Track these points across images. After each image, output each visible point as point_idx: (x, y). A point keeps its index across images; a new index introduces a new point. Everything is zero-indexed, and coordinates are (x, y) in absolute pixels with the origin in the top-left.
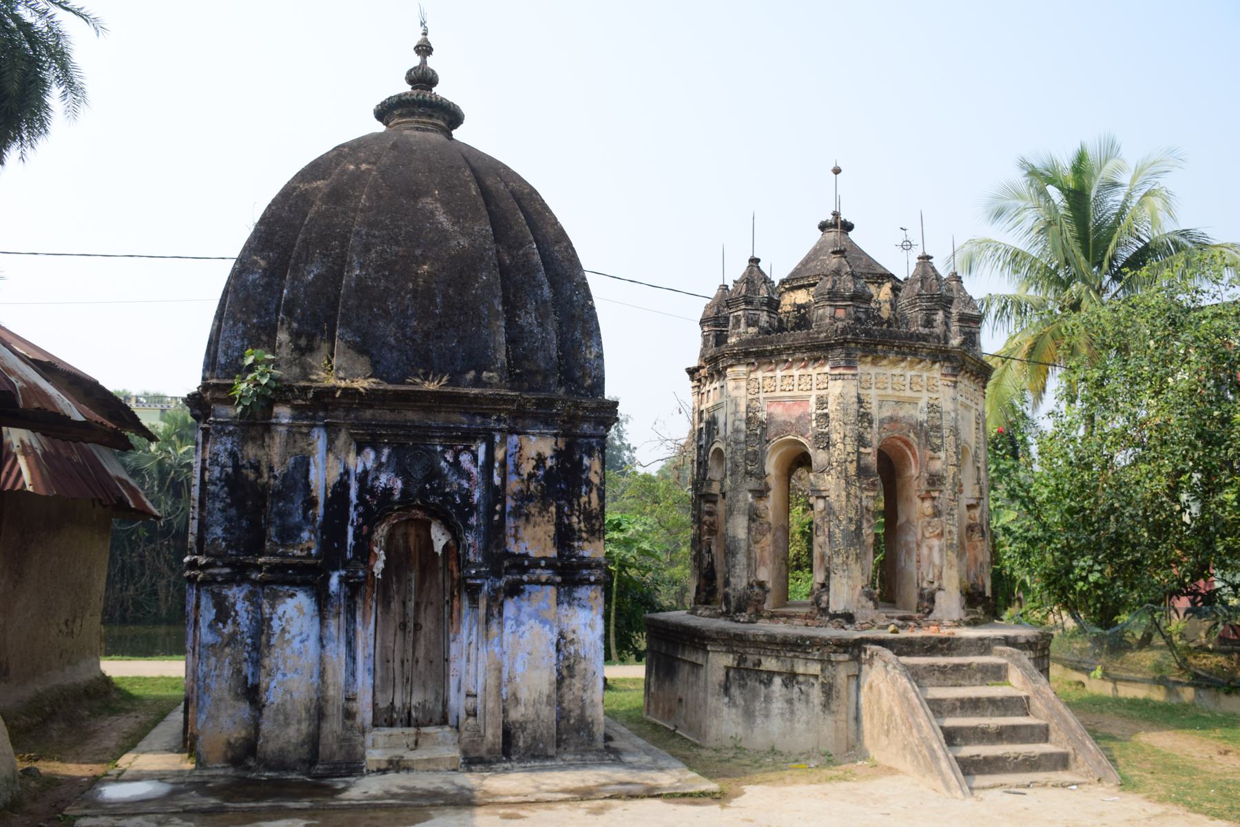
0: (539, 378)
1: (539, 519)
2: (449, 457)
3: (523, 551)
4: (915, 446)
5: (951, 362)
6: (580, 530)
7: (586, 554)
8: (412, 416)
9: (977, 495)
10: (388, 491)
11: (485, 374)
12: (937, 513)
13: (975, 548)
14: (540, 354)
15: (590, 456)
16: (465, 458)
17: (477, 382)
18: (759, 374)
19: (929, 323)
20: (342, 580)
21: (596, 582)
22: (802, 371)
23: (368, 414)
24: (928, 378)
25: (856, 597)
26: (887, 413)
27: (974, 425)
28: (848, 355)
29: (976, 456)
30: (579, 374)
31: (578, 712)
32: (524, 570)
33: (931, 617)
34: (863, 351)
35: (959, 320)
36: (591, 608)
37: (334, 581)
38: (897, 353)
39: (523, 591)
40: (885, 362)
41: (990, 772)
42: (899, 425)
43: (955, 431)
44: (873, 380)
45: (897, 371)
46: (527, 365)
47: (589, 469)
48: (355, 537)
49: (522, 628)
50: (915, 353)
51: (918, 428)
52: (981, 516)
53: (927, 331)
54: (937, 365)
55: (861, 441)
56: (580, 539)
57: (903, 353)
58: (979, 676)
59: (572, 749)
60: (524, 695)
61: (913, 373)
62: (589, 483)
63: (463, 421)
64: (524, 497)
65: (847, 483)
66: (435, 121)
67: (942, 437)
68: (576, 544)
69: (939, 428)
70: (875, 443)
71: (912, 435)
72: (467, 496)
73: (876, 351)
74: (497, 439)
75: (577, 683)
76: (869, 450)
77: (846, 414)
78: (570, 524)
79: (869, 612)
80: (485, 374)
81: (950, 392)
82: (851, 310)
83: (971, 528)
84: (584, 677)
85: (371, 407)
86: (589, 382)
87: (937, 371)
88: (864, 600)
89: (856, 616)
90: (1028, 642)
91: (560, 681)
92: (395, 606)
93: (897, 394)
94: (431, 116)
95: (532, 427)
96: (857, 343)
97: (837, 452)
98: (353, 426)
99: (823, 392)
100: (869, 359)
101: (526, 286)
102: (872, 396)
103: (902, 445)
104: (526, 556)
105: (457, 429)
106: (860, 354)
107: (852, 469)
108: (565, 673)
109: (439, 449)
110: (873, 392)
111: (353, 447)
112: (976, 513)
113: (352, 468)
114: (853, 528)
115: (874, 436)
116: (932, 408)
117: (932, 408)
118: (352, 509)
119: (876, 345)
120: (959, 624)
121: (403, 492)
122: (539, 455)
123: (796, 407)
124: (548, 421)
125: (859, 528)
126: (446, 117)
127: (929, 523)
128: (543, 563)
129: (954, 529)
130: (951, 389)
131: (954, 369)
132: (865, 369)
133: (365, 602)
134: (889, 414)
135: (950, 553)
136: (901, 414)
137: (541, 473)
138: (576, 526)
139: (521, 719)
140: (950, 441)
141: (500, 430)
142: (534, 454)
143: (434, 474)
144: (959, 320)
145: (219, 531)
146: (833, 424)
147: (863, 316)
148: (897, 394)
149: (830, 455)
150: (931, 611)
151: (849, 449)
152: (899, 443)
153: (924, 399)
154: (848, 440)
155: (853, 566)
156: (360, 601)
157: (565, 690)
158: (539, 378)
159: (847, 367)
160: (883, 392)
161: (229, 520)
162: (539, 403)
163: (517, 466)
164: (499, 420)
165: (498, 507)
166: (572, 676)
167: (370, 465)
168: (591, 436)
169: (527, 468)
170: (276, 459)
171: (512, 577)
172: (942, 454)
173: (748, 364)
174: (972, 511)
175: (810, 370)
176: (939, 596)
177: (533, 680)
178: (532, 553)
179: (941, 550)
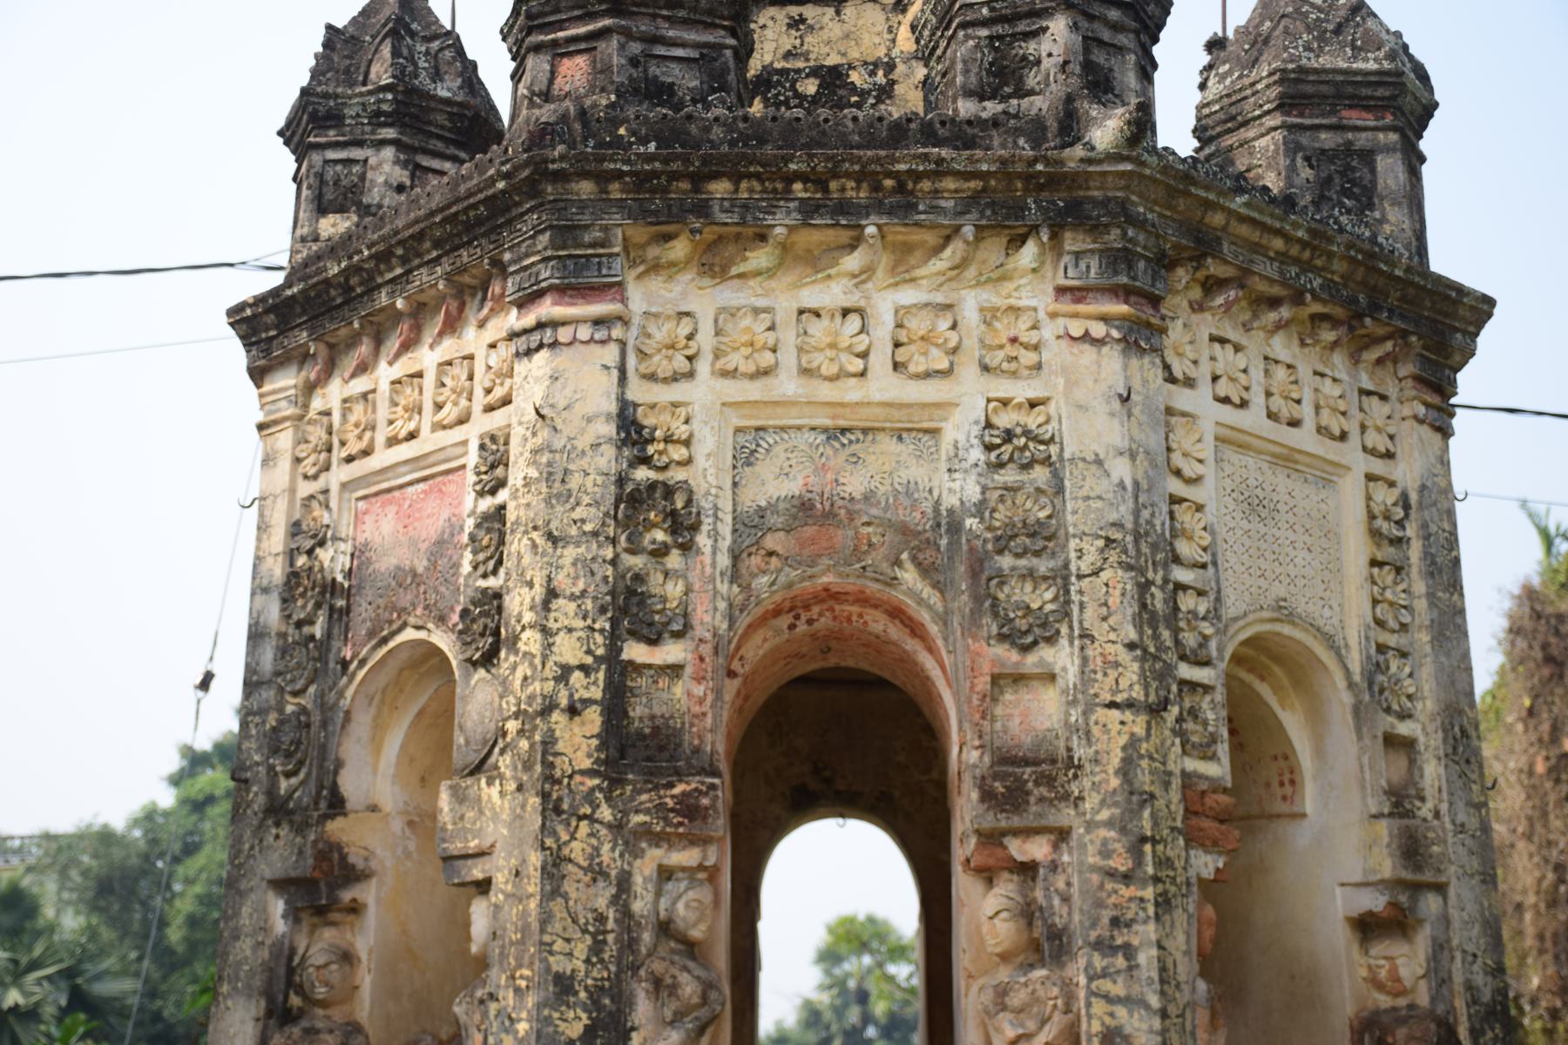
4: (934, 629)
5: (1096, 229)
9: (1387, 867)
12: (1045, 944)
18: (333, 394)
19: (1004, 75)
22: (449, 348)
24: (989, 315)
26: (776, 482)
27: (1356, 550)
28: (566, 233)
29: (1376, 690)
34: (641, 214)
35: (1283, 106)
38: (809, 210)
40: (760, 258)
42: (843, 537)
43: (1150, 548)
44: (705, 339)
45: (830, 293)
50: (900, 201)
51: (933, 540)
52: (1437, 973)
53: (992, 108)
54: (1028, 253)
55: (631, 610)
65: (552, 808)
67: (1062, 578)
69: (1042, 536)
70: (708, 617)
71: (909, 576)
73: (703, 209)
76: (671, 652)
81: (1111, 367)
82: (610, 49)
93: (826, 392)
96: (603, 179)
97: (521, 675)
99: (498, 419)
100: (679, 248)
103: (895, 632)
106: (622, 228)
107: (578, 742)
110: (703, 392)
112: (1408, 960)
119: (698, 180)
123: (431, 505)
127: (1002, 992)
131: (1118, 259)
132: (668, 296)
134: (793, 487)
136: (855, 484)
144: (1283, 106)
146: (517, 545)
148: (826, 392)
149: (506, 690)
151: (568, 650)
152: (878, 623)
153: (967, 404)
154: (565, 610)
159: (567, 291)
160: (753, 391)
172: (1062, 657)
173: (305, 358)
174: (1379, 949)
175: (472, 339)
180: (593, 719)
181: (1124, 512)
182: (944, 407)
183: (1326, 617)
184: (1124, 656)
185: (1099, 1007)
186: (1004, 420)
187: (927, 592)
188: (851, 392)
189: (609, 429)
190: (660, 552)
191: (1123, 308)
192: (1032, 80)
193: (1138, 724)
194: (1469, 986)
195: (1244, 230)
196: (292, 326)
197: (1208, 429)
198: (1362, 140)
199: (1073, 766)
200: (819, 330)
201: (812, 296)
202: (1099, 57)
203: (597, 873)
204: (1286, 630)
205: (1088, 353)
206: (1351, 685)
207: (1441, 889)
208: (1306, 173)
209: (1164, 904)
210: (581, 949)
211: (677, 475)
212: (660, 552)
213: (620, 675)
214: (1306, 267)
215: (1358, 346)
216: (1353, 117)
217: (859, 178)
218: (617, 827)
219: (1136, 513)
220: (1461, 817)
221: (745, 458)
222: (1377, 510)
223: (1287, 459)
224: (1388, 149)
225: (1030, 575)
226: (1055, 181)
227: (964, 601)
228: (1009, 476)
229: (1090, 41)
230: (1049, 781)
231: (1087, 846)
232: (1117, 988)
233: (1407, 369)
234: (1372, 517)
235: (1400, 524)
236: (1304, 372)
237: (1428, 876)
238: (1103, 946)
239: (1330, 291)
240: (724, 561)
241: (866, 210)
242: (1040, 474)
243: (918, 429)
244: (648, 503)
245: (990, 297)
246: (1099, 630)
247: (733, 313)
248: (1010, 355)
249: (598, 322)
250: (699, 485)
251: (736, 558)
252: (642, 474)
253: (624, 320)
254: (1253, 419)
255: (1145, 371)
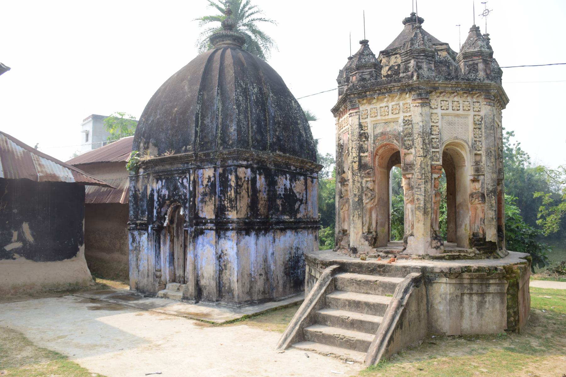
0: (209, 144)
1: (209, 203)
2: (180, 181)
3: (204, 217)
6: (228, 207)
7: (230, 217)
8: (168, 167)
10: (165, 195)
11: (188, 147)
13: (476, 209)
14: (210, 134)
15: (231, 174)
16: (185, 181)
17: (186, 150)
20: (152, 228)
21: (232, 229)
23: (157, 168)
24: (404, 104)
25: (358, 239)
26: (379, 131)
28: (351, 102)
29: (474, 147)
30: (227, 139)
31: (228, 285)
32: (205, 224)
33: (405, 252)
34: (359, 98)
36: (232, 241)
37: (150, 229)
38: (379, 94)
39: (204, 233)
40: (374, 101)
41: (326, 343)
42: (387, 137)
44: (369, 112)
45: (384, 104)
46: (206, 140)
47: (231, 180)
48: (157, 213)
49: (205, 248)
50: (390, 91)
51: (397, 136)
52: (482, 187)
55: (361, 149)
56: (228, 210)
57: (383, 93)
58: (381, 289)
59: (226, 300)
60: (205, 275)
61: (393, 103)
62: (231, 186)
63: (181, 166)
64: (205, 194)
66: (225, 42)
67: (413, 140)
68: (226, 213)
69: (410, 134)
70: (370, 149)
71: (395, 141)
72: (185, 196)
73: (366, 96)
74: (191, 172)
75: (228, 272)
76: (366, 154)
77: (353, 136)
78: (224, 205)
79: (366, 247)
80: (188, 147)
81: (419, 110)
82: (357, 75)
83: (472, 195)
84: (230, 270)
85: (157, 166)
86: (231, 142)
87: (408, 99)
88: (363, 240)
89: (358, 249)
90: (442, 272)
91: (221, 271)
92: (180, 238)
93: (384, 118)
94: (223, 41)
95: (207, 165)
96: (354, 94)
98: (153, 173)
100: (365, 101)
101: (210, 107)
102: (369, 122)
104: (205, 218)
105: (180, 170)
106: (357, 100)
107: (356, 166)
108: (223, 267)
109: (178, 178)
110: (369, 120)
111: (155, 181)
112: (478, 185)
113: (155, 188)
114: (356, 199)
115: (369, 145)
116: (407, 122)
117: (407, 122)
118: (155, 203)
119: (365, 92)
120: (423, 258)
121: (168, 195)
122: (209, 176)
124: (211, 161)
125: (361, 200)
126: (229, 38)
128: (209, 221)
129: (422, 198)
130: (420, 108)
131: (420, 94)
132: (365, 107)
133: (165, 236)
134: (381, 131)
135: (417, 212)
136: (388, 130)
137: (209, 184)
138: (226, 205)
139: (205, 285)
140: (418, 142)
141: (191, 168)
142: (207, 176)
143: (176, 188)
145: (132, 213)
147: (368, 77)
148: (384, 118)
150: (405, 249)
153: (401, 116)
155: (357, 221)
156: (162, 237)
157: (223, 275)
158: (209, 144)
159: (353, 109)
160: (375, 119)
161: (134, 209)
162: (205, 155)
163: (202, 182)
164: (191, 164)
165: (192, 199)
166: (226, 269)
167: (160, 186)
168: (231, 166)
169: (205, 182)
170: (140, 187)
171: (198, 226)
172: (413, 150)
176: (410, 239)
177: (208, 269)
178: (208, 217)
179: (412, 211)
180: (357, 163)
181: (421, 130)
182: (398, 118)
183: (465, 138)
184: (421, 150)
185: (416, 195)
186: (406, 119)
187: (397, 143)
188: (387, 117)
189: (358, 126)
190: (364, 141)
191: (420, 101)
192: (410, 70)
193: (422, 159)
194: (487, 188)
195: (443, 85)
196: (336, 111)
197: (440, 115)
198: (476, 62)
199: (413, 164)
200: (382, 109)
201: (382, 105)
202: (419, 64)
203: (358, 182)
204: (456, 141)
205: (416, 108)
206: (469, 147)
207: (484, 175)
208: (467, 68)
209: (426, 182)
210: (357, 191)
211: (366, 131)
212: (364, 141)
213: (360, 158)
214: (456, 87)
215: (473, 95)
216: (475, 58)
217: (384, 89)
218: (360, 176)
219: (423, 130)
220: (488, 164)
221: (375, 128)
222: (475, 120)
223: (458, 116)
224: (480, 62)
225: (409, 140)
226: (409, 85)
227: (401, 144)
228: (406, 127)
229: (417, 63)
230: (411, 167)
231: (416, 174)
232: (419, 193)
233: (483, 97)
234: (474, 121)
235: (481, 121)
236: (461, 102)
237: (480, 173)
238: (417, 188)
239: (462, 89)
240: (372, 142)
241: (386, 93)
242: (410, 126)
243: (395, 121)
244: (363, 136)
245: (404, 102)
246: (417, 147)
247: (372, 109)
248: (407, 110)
249: (356, 112)
250: (368, 132)
251: (374, 141)
252: (362, 131)
253: (359, 112)
254: (450, 111)
255: (427, 109)
